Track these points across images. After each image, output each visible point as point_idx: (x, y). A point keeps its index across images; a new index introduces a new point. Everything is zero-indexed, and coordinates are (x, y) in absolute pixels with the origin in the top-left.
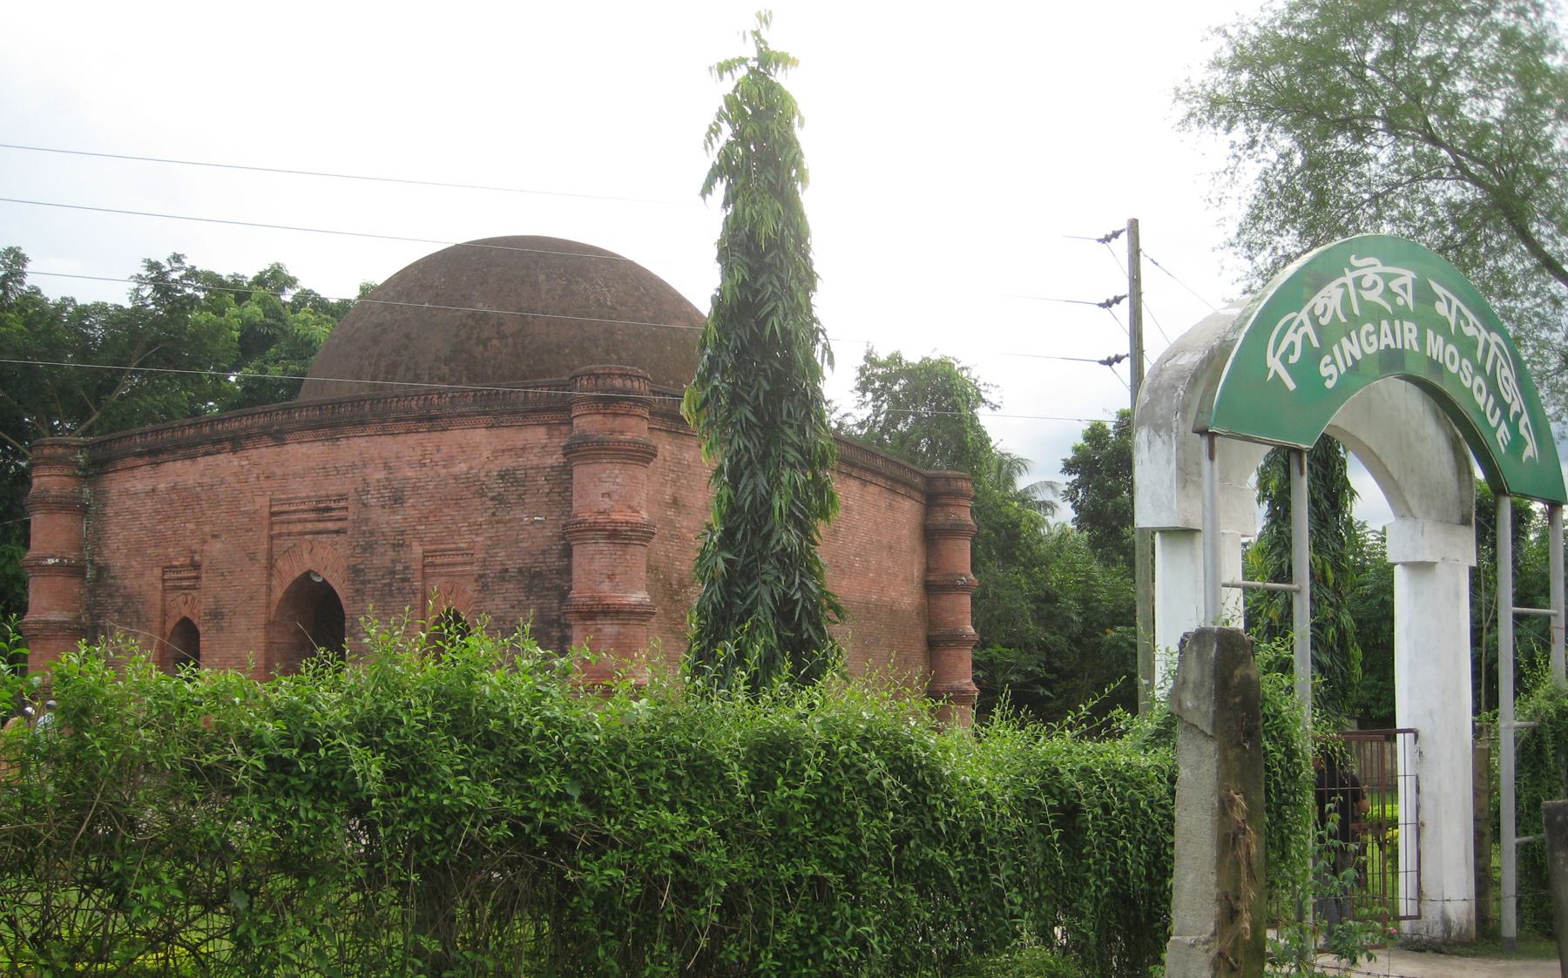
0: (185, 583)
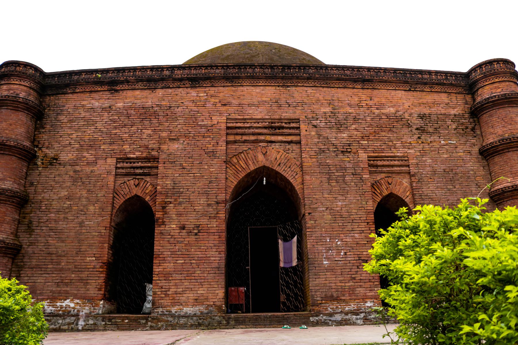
0: (138, 171)
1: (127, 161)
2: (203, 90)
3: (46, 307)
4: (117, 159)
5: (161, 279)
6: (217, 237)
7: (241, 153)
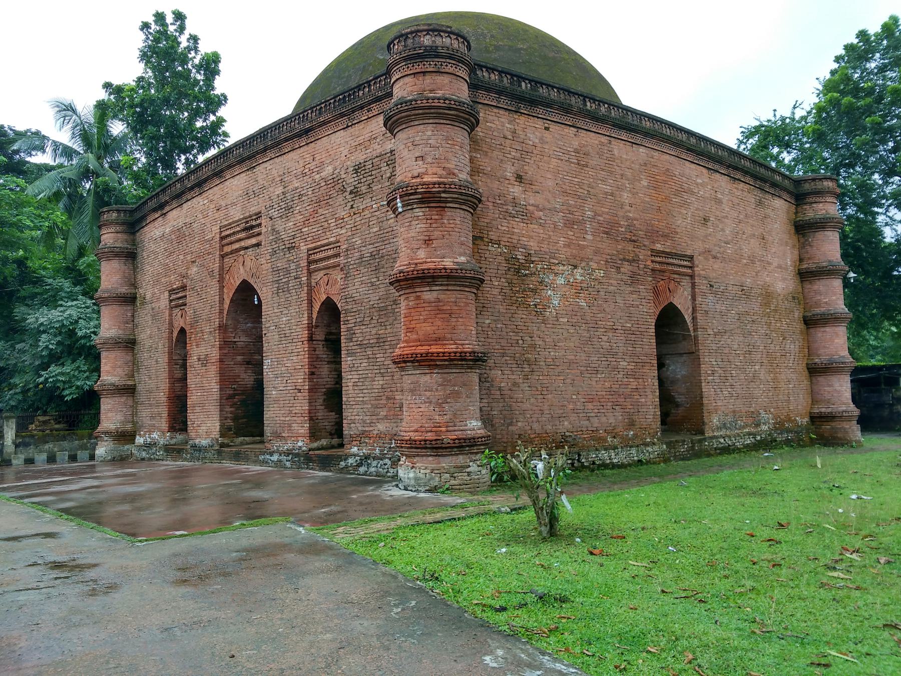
4: (170, 291)
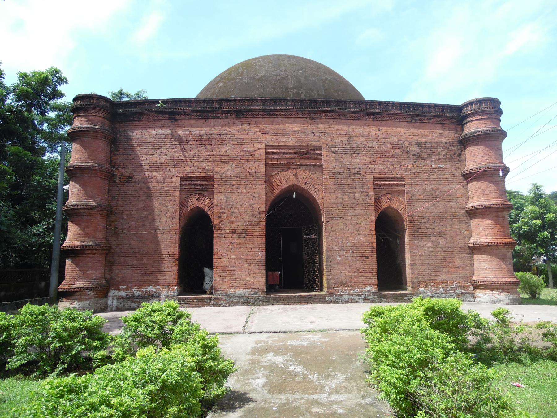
1: (189, 179)
2: (246, 120)
3: (135, 292)
4: (181, 178)
5: (219, 270)
6: (260, 239)
7: (277, 173)
